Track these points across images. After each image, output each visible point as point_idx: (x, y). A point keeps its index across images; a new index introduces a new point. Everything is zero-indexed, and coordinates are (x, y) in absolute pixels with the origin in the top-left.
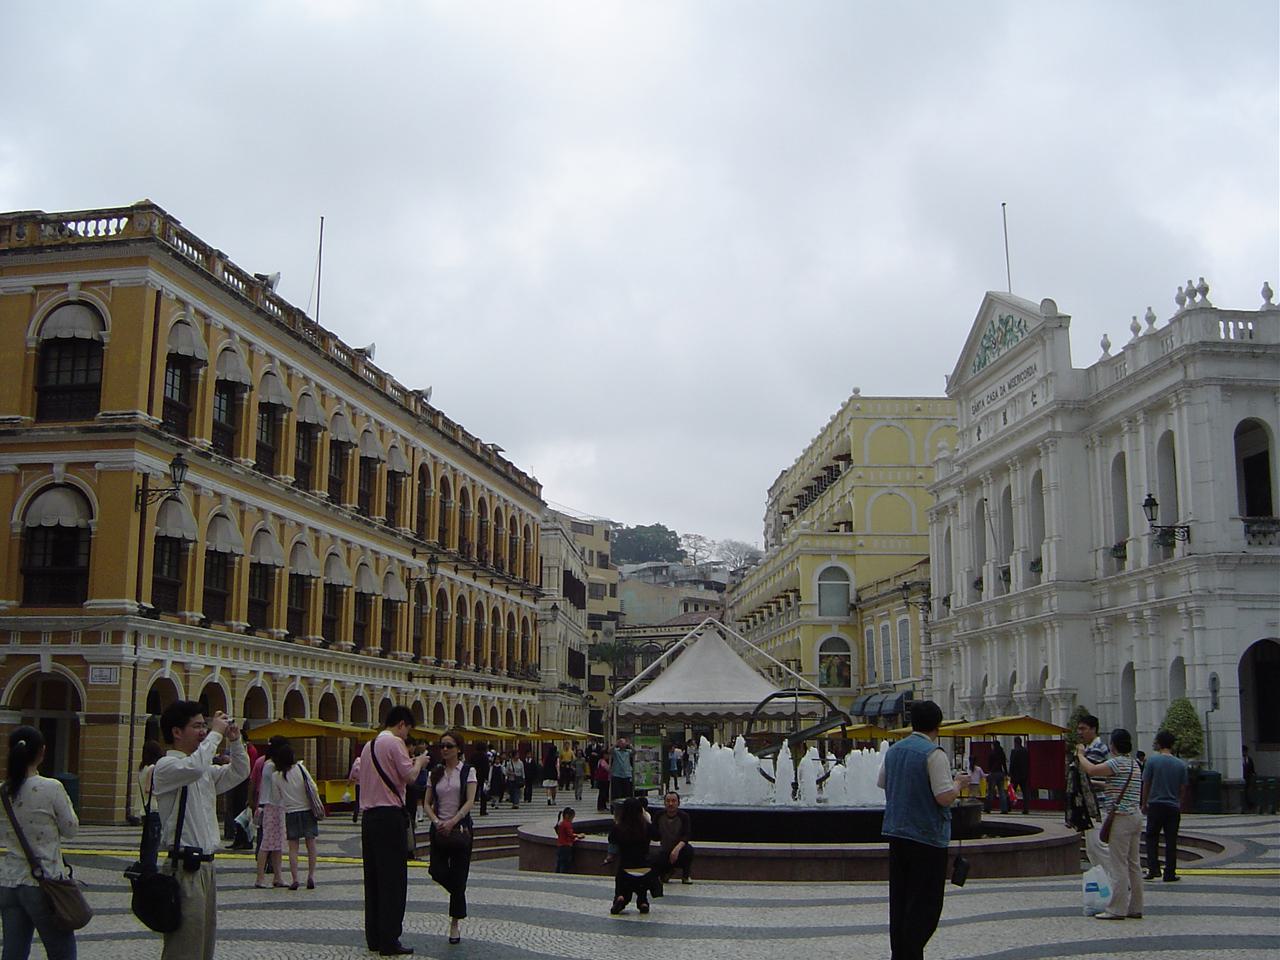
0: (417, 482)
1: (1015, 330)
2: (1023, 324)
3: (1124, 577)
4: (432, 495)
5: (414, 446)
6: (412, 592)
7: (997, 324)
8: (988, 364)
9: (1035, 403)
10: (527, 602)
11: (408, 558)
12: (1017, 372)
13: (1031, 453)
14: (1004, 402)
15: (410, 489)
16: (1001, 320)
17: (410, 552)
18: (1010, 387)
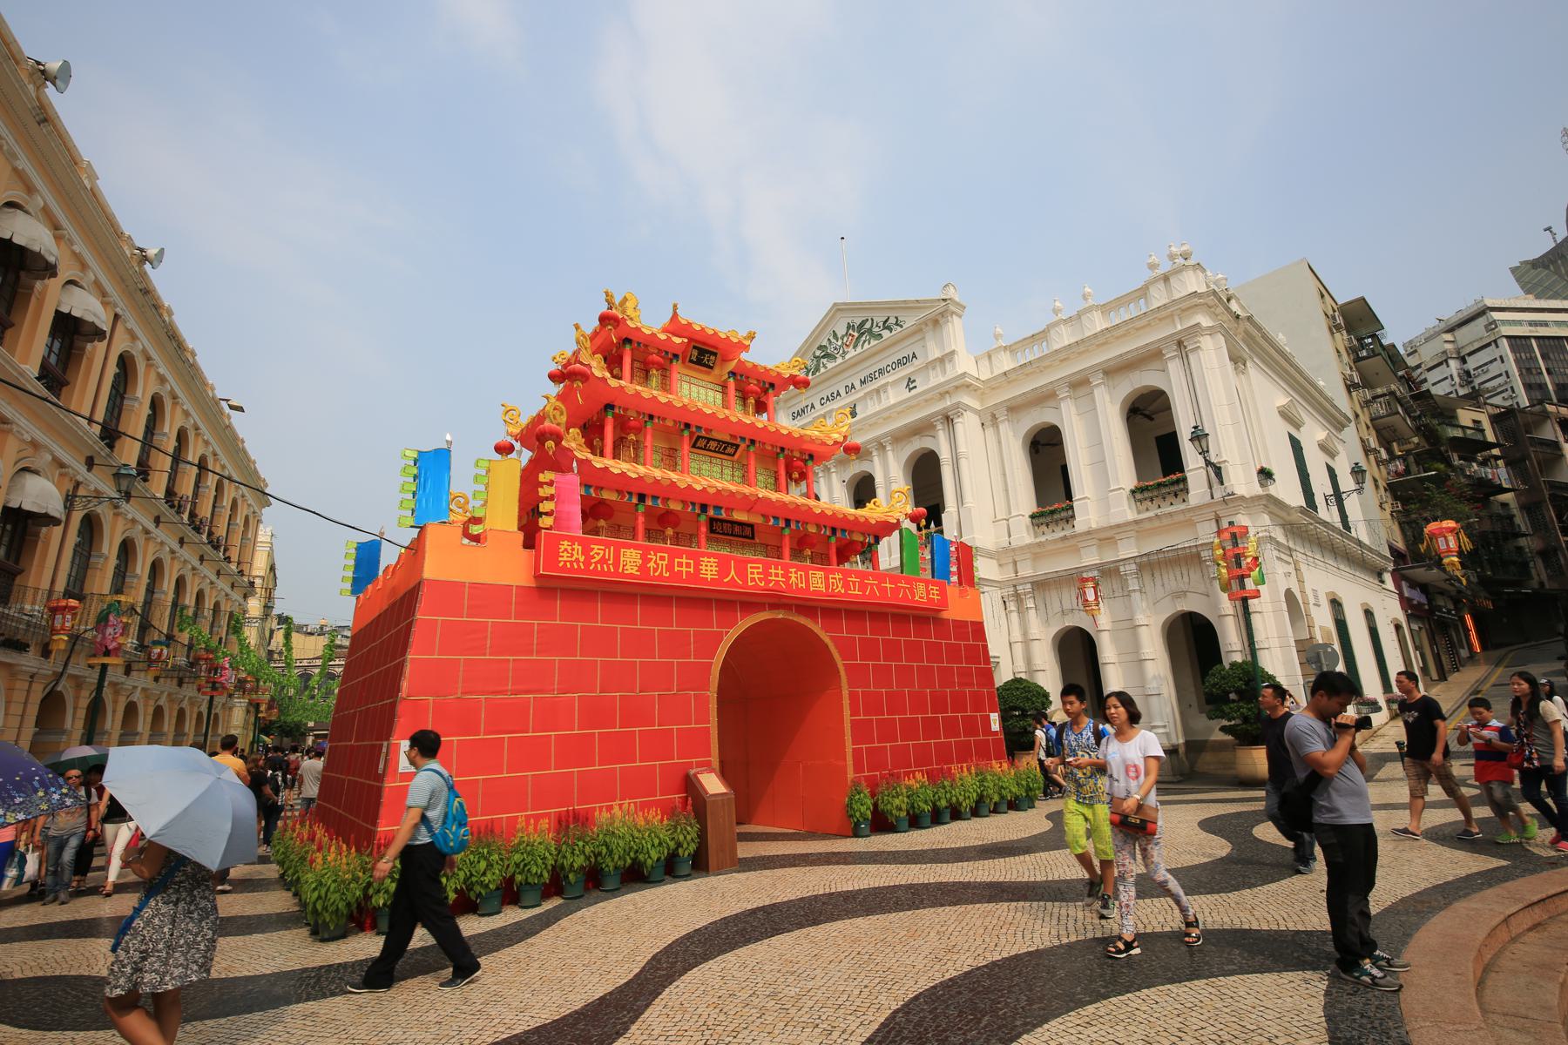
0: (112, 369)
1: (875, 330)
2: (892, 320)
3: (1073, 537)
4: (136, 405)
5: (118, 310)
6: (77, 516)
7: (841, 331)
8: (822, 370)
9: (910, 390)
10: (236, 596)
11: (83, 469)
12: (882, 365)
13: (923, 428)
14: (861, 394)
15: (98, 364)
16: (849, 327)
17: (83, 460)
18: (863, 382)
